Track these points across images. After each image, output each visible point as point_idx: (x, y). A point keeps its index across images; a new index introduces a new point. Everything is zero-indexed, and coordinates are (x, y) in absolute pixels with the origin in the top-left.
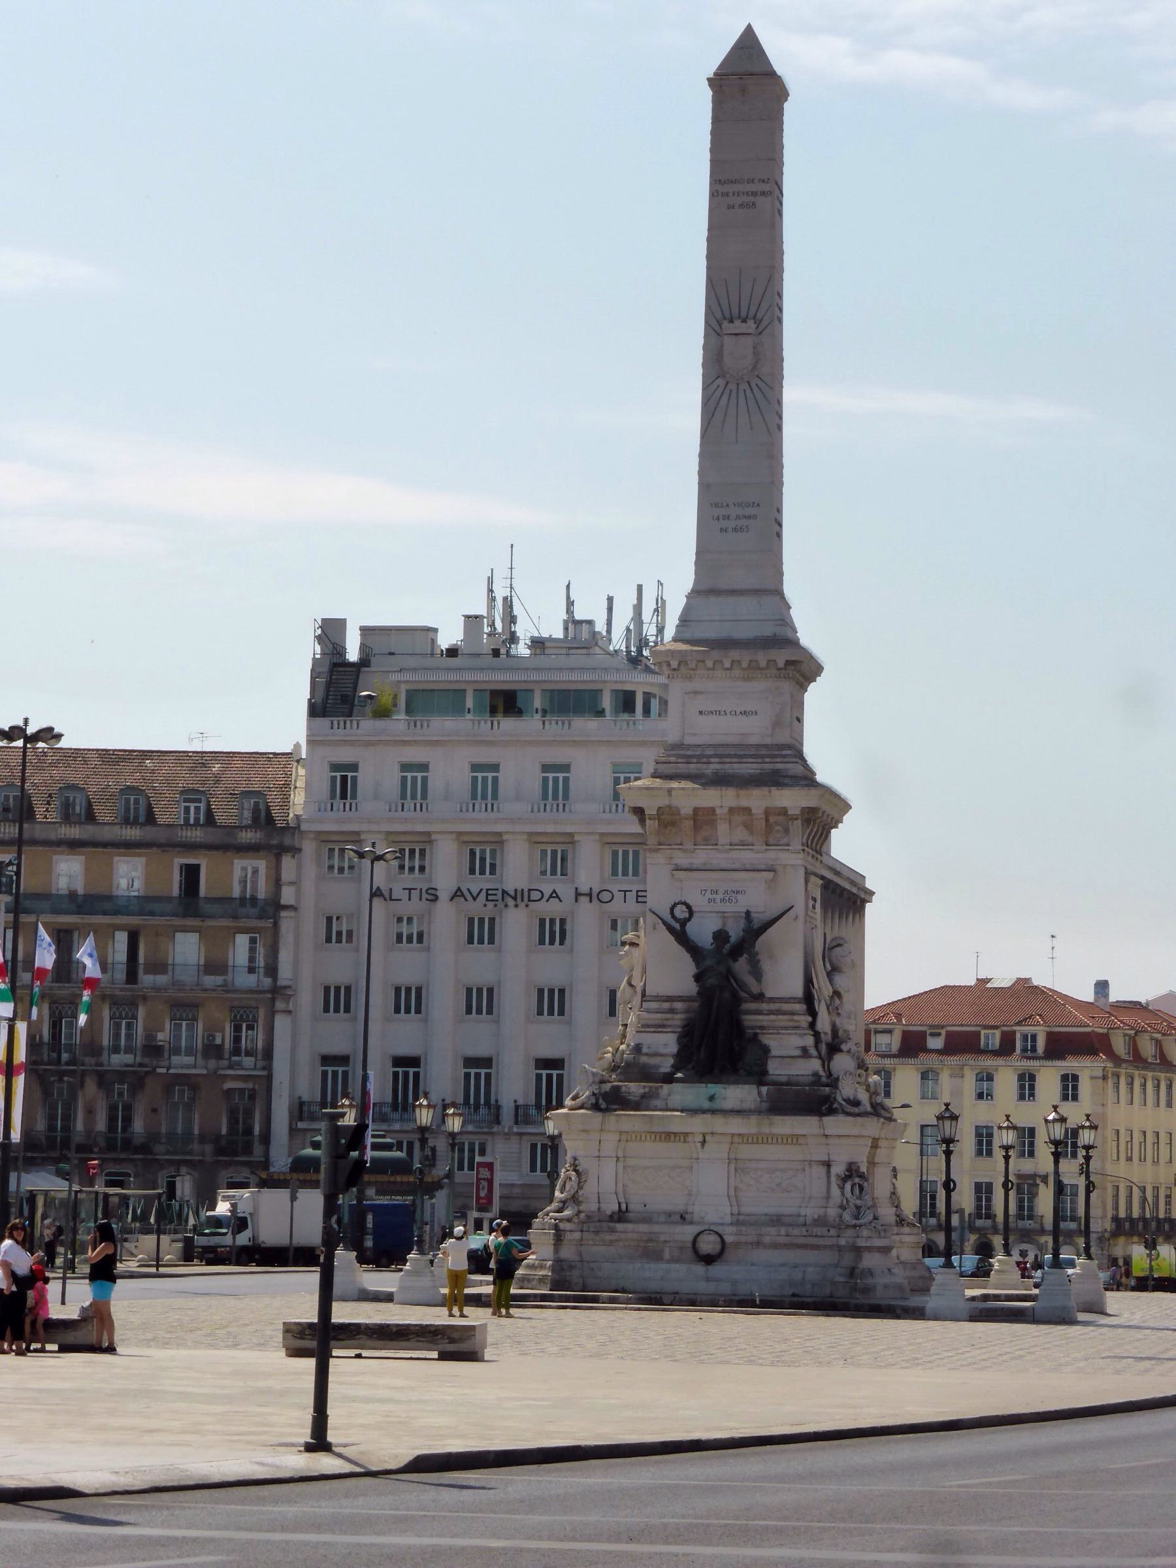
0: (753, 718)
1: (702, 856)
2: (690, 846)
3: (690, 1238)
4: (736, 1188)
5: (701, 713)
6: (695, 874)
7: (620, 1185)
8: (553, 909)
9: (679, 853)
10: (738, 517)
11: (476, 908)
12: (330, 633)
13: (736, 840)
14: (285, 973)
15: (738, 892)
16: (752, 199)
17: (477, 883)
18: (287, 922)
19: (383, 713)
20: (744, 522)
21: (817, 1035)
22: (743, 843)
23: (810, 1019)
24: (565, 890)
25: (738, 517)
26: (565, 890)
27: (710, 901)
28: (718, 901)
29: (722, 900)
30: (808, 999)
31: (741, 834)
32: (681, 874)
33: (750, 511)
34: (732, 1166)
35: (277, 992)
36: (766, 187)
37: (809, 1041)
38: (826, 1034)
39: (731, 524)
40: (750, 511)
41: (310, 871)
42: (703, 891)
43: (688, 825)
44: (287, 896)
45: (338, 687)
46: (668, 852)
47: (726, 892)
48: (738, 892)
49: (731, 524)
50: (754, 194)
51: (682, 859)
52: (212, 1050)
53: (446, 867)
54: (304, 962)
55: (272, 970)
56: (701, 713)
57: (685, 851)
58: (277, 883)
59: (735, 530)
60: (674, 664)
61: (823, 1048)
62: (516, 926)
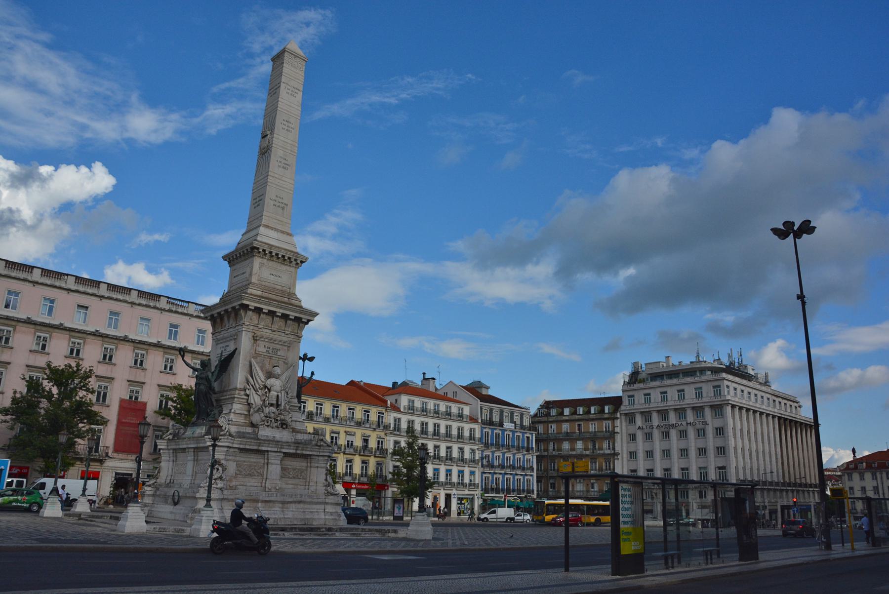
8: (681, 428)
11: (663, 429)
12: (635, 364)
14: (617, 449)
17: (664, 423)
18: (618, 438)
19: (640, 382)
24: (684, 423)
26: (684, 423)
35: (615, 455)
41: (624, 424)
44: (617, 430)
45: (635, 377)
52: (601, 469)
53: (656, 420)
54: (621, 445)
55: (614, 449)
58: (614, 427)
62: (673, 433)
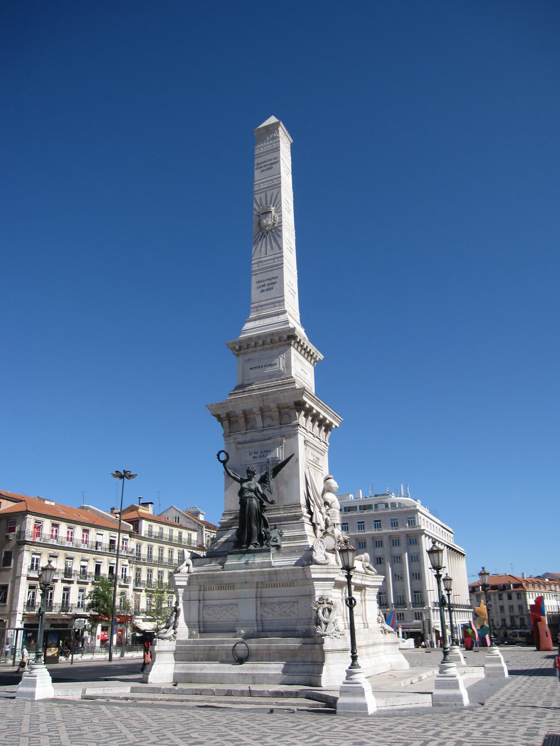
0: (273, 367)
1: (249, 436)
2: (244, 431)
3: (232, 648)
4: (261, 615)
5: (251, 369)
6: (246, 445)
7: (201, 617)
9: (240, 436)
10: (268, 285)
13: (265, 425)
15: (267, 451)
16: (271, 166)
20: (271, 286)
21: (314, 525)
22: (269, 426)
23: (310, 516)
25: (268, 285)
27: (254, 458)
28: (258, 457)
29: (260, 456)
30: (308, 505)
31: (268, 422)
32: (240, 446)
33: (273, 281)
34: (259, 602)
36: (276, 160)
37: (308, 528)
38: (318, 524)
39: (266, 288)
40: (273, 281)
42: (250, 454)
43: (242, 421)
46: (234, 436)
47: (261, 452)
48: (267, 451)
49: (266, 288)
50: (272, 164)
51: (240, 438)
56: (251, 369)
57: (242, 434)
59: (268, 290)
60: (237, 347)
61: (319, 534)
